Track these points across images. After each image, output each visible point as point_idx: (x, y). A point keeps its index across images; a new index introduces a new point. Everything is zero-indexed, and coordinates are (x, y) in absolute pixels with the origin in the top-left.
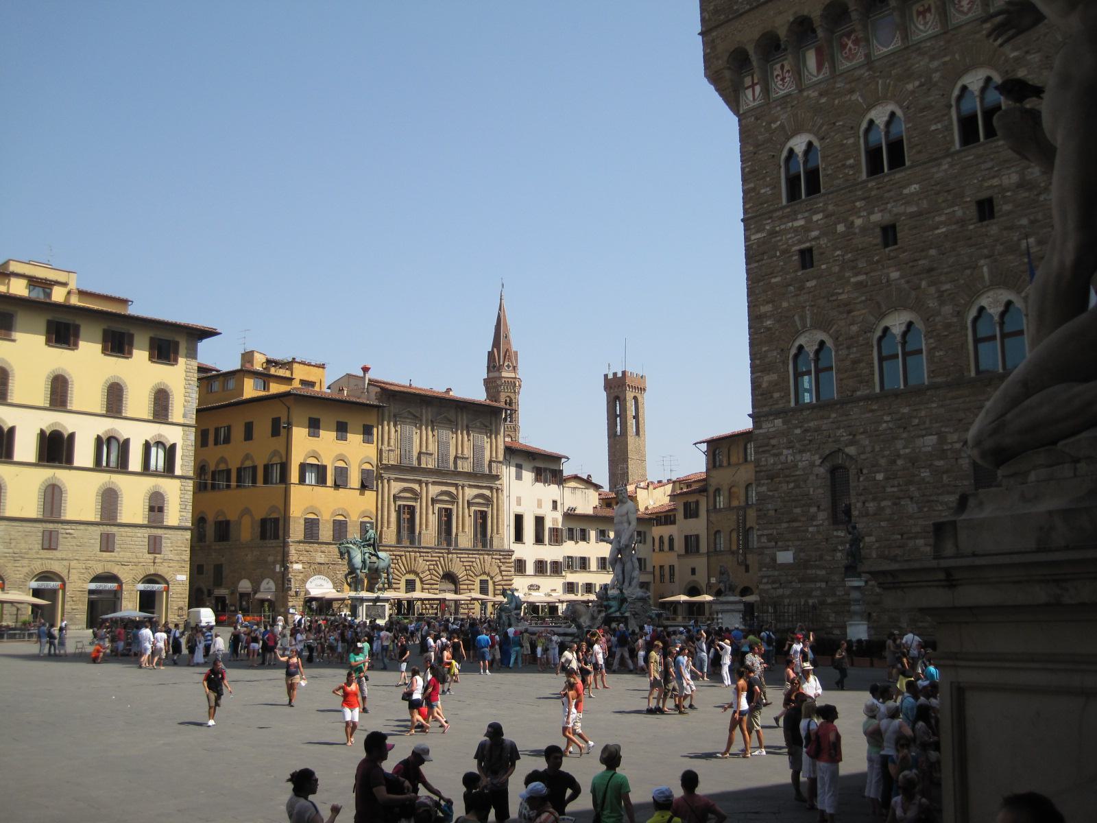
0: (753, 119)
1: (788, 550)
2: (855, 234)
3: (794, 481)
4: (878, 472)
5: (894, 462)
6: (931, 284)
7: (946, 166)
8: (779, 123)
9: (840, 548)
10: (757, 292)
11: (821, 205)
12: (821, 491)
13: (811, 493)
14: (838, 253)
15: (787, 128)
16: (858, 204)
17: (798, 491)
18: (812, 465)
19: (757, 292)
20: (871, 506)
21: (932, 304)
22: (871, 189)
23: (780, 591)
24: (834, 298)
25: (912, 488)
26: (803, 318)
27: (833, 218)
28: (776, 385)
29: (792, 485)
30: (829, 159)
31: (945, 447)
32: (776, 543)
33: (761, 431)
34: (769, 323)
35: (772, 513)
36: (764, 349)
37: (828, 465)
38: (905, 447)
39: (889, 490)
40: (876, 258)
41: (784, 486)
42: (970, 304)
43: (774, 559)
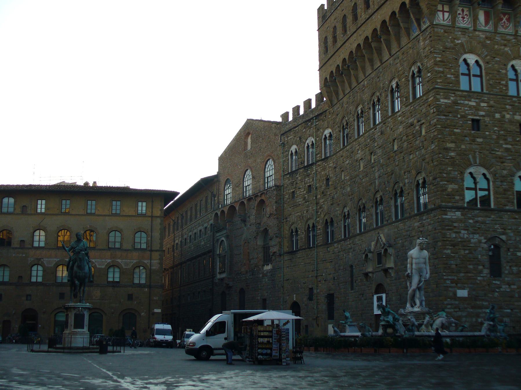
0: (442, 31)
2: (505, 122)
3: (469, 250)
8: (460, 41)
9: (497, 290)
10: (445, 133)
11: (486, 99)
12: (485, 257)
13: (479, 256)
14: (496, 129)
15: (465, 47)
16: (507, 106)
17: (471, 255)
18: (480, 242)
19: (445, 133)
22: (515, 102)
23: (460, 313)
24: (494, 152)
26: (474, 158)
27: (493, 109)
28: (457, 192)
29: (467, 252)
30: (491, 75)
32: (456, 284)
33: (447, 217)
34: (452, 154)
35: (454, 266)
36: (449, 169)
40: (518, 139)
41: (462, 252)
43: (455, 294)
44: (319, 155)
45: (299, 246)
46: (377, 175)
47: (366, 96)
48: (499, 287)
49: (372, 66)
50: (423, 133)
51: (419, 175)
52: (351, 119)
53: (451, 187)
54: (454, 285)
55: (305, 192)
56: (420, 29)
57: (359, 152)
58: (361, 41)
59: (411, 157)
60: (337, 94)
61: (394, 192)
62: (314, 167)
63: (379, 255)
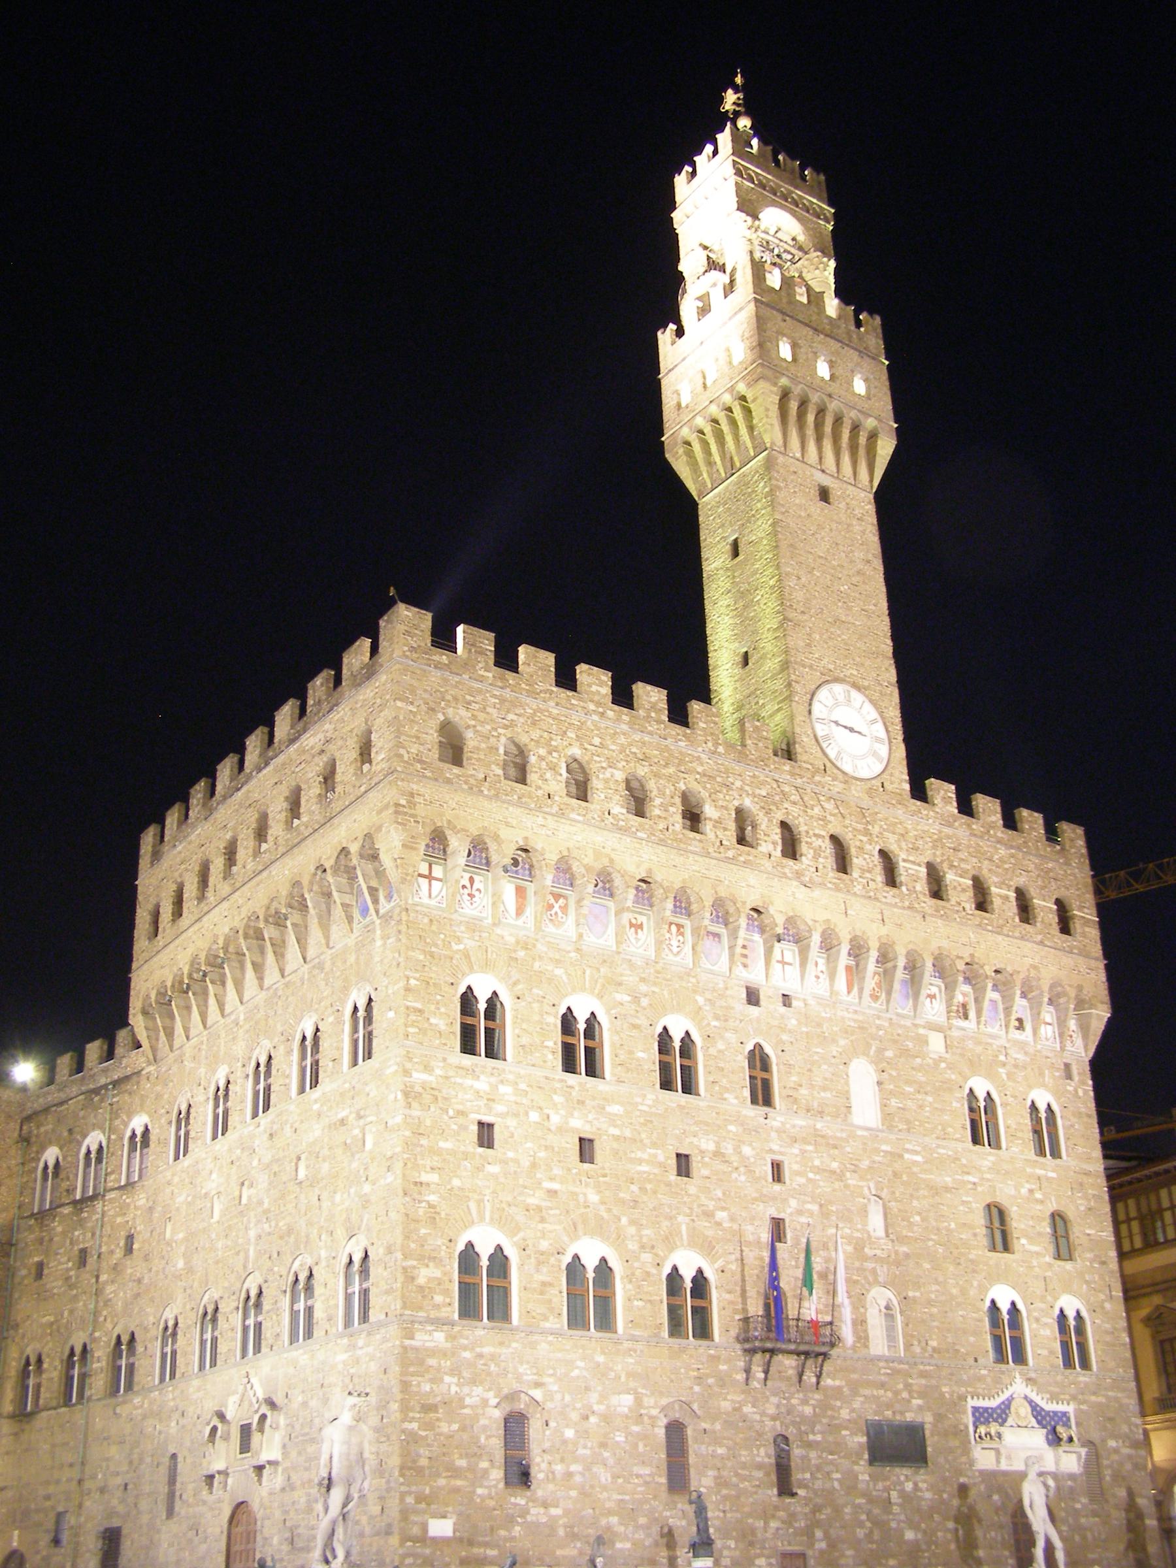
0: (426, 920)
1: (444, 1517)
4: (567, 1426)
5: (587, 1418)
6: (632, 1222)
7: (650, 1103)
8: (461, 947)
9: (519, 1520)
13: (483, 1439)
14: (529, 1145)
15: (473, 959)
16: (555, 1097)
17: (465, 1436)
18: (485, 1402)
20: (559, 1468)
21: (632, 1246)
25: (606, 1454)
31: (643, 1411)
32: (428, 1504)
33: (413, 1342)
34: (433, 1198)
36: (423, 1231)
37: (507, 1408)
38: (600, 1402)
39: (581, 1451)
42: (665, 1258)
44: (113, 1177)
45: (41, 1402)
46: (252, 1234)
47: (239, 1049)
48: (524, 1512)
49: (260, 979)
50: (369, 1145)
51: (354, 1239)
52: (202, 1098)
53: (425, 1274)
54: (423, 1505)
55: (70, 1264)
56: (377, 912)
57: (214, 1176)
58: (238, 922)
59: (338, 1197)
60: (170, 1034)
61: (291, 1278)
62: (99, 1205)
63: (246, 1431)
